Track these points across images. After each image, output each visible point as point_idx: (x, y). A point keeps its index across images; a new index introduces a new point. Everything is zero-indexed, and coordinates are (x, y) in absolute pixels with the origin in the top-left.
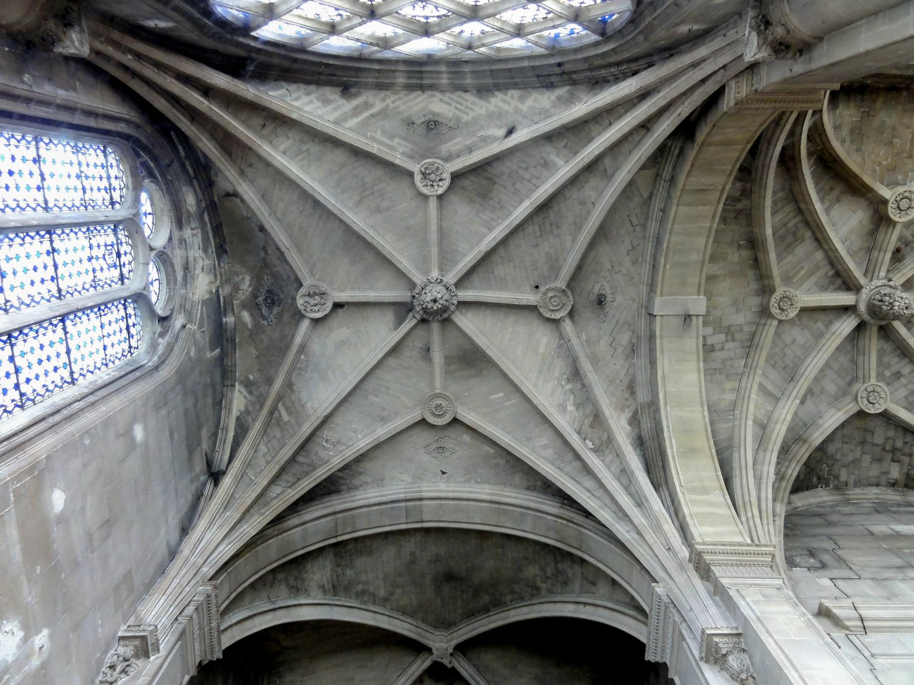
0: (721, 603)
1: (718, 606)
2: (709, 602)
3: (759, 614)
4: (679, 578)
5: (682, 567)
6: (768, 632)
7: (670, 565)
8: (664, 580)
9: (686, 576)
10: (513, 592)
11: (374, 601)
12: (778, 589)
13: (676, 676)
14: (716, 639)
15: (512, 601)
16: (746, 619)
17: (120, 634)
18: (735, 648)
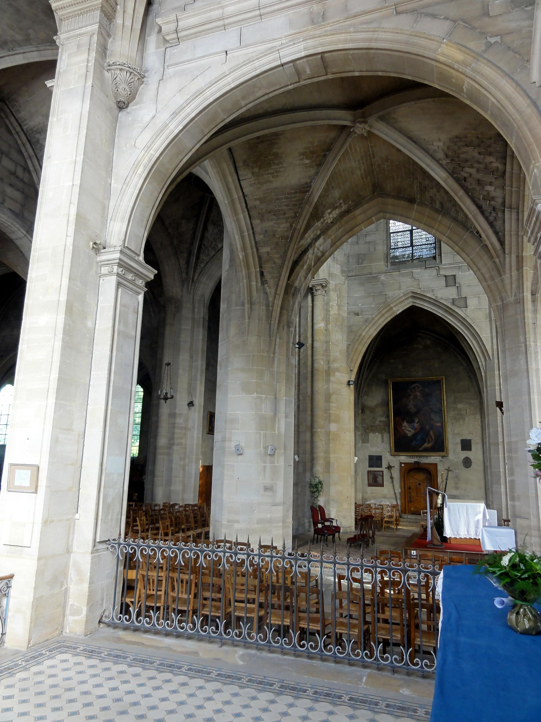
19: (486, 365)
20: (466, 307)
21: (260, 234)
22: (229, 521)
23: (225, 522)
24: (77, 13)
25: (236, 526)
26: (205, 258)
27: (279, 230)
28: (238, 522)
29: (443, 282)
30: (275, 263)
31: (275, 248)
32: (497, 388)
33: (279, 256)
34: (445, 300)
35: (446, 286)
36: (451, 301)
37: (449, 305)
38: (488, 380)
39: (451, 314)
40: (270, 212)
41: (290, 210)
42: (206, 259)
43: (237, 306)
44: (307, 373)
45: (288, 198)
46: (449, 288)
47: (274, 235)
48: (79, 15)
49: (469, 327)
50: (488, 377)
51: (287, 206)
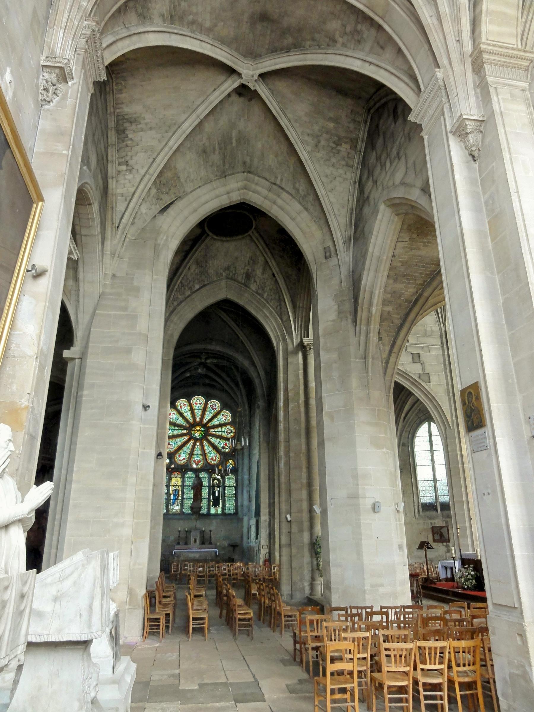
0: (479, 94)
1: (477, 97)
2: (472, 93)
3: (503, 110)
4: (457, 68)
5: (462, 59)
6: (504, 124)
7: (455, 56)
8: (445, 67)
9: (462, 67)
10: (313, 39)
11: (201, 30)
12: (523, 90)
13: (426, 135)
14: (467, 122)
15: (310, 47)
16: (493, 112)
17: (42, 63)
18: (476, 129)
19: (446, 433)
20: (430, 382)
21: (389, 293)
22: (372, 586)
23: (367, 587)
24: (502, 63)
25: (381, 590)
26: (179, 297)
27: (406, 293)
28: (382, 585)
29: (410, 359)
30: (393, 322)
31: (397, 309)
32: (459, 453)
33: (399, 316)
34: (414, 374)
35: (413, 362)
36: (418, 375)
37: (417, 379)
38: (449, 446)
39: (417, 387)
40: (405, 275)
41: (421, 277)
42: (181, 297)
43: (356, 359)
44: (300, 430)
45: (424, 267)
46: (416, 364)
47: (400, 297)
48: (503, 66)
49: (432, 399)
50: (448, 443)
51: (421, 273)
